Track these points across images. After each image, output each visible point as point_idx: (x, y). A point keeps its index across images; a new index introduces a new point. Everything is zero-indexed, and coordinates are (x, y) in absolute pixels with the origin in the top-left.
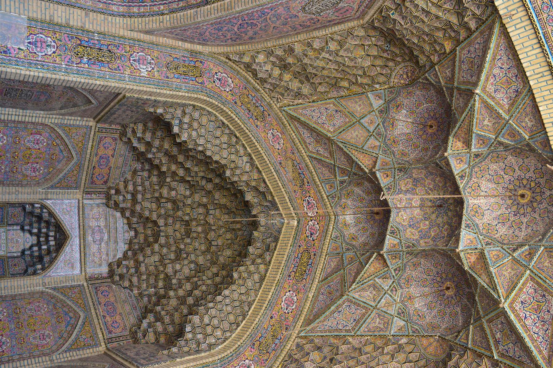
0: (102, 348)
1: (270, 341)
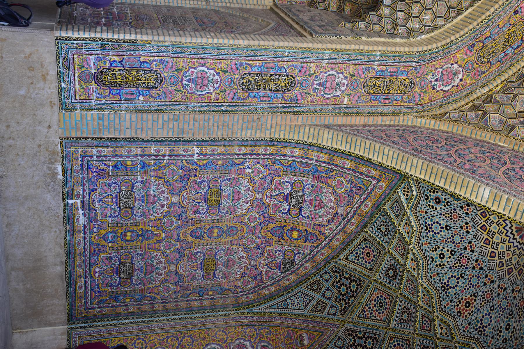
1: (499, 47)
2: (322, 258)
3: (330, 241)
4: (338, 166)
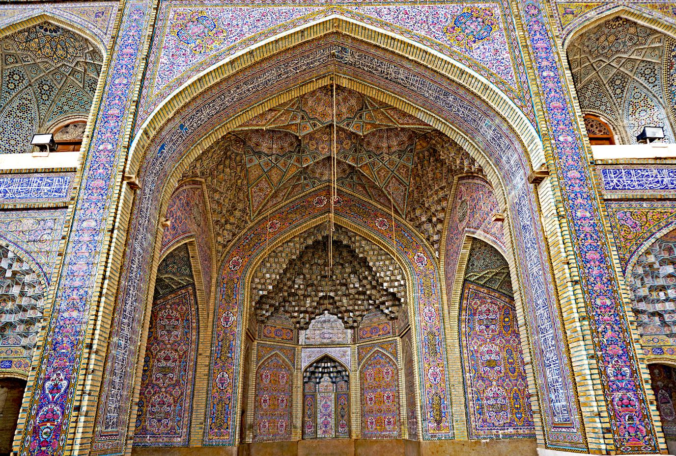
0: (398, 339)
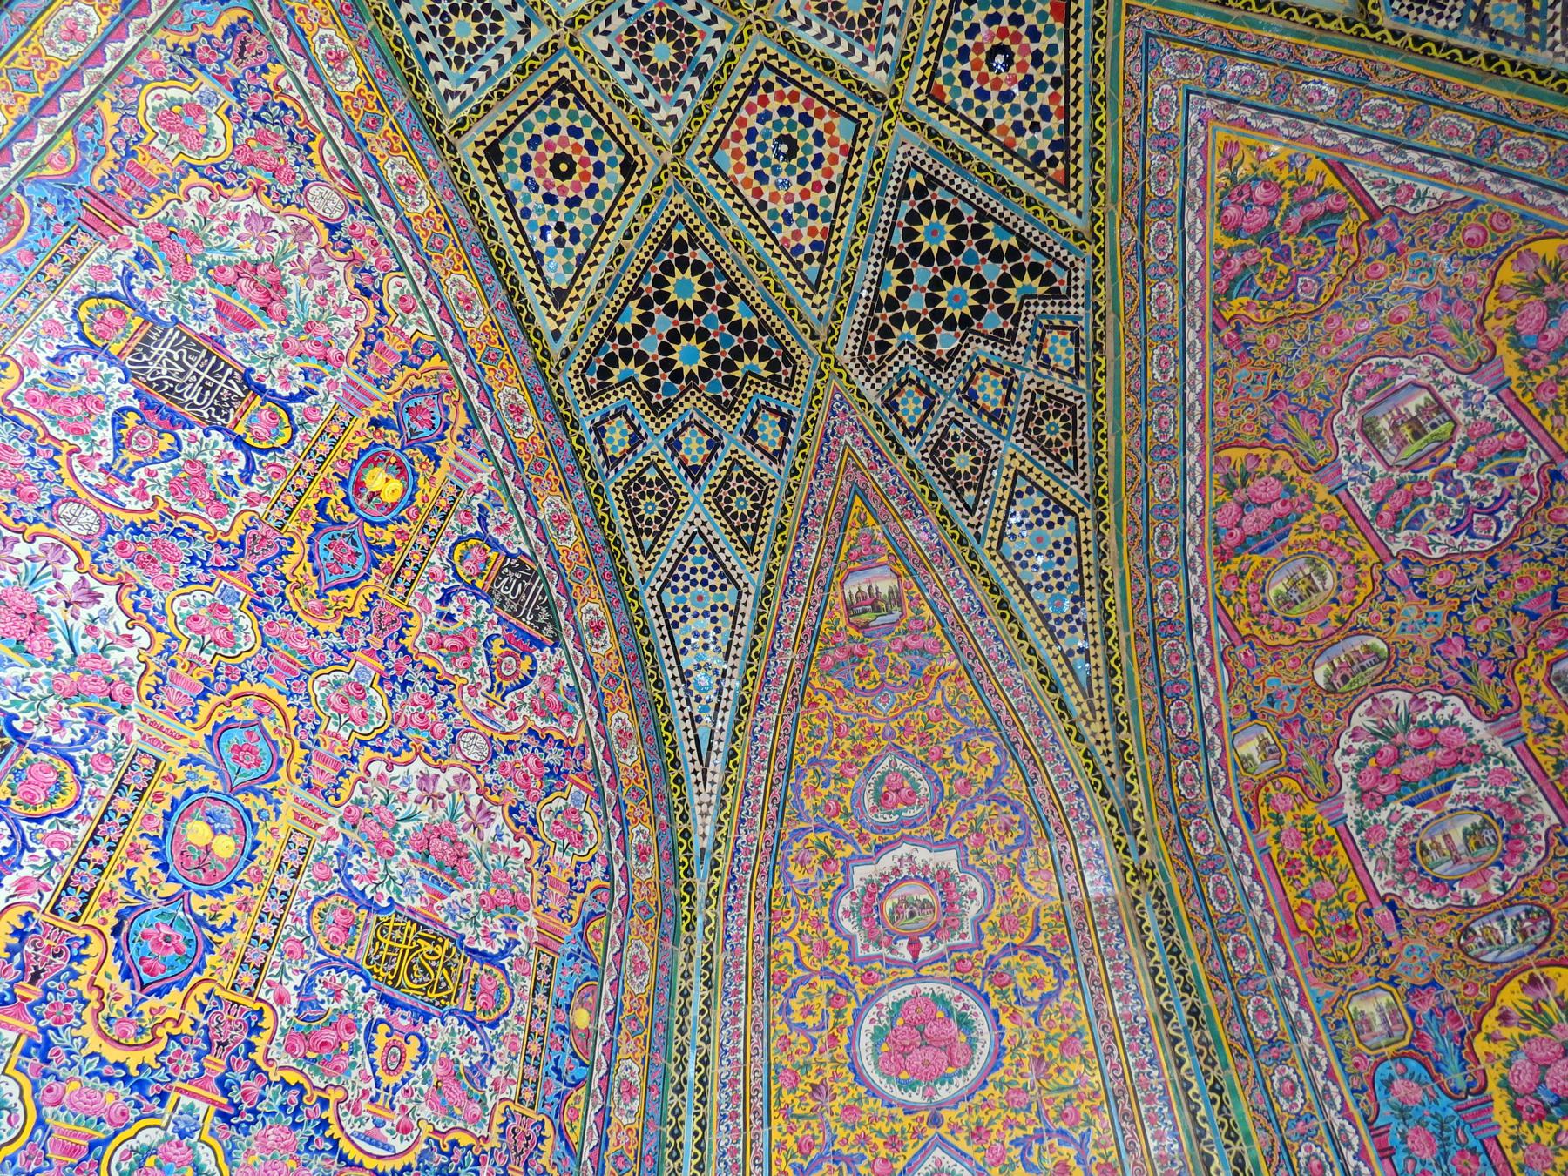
2: (530, 418)
3: (460, 337)
4: (77, 74)
